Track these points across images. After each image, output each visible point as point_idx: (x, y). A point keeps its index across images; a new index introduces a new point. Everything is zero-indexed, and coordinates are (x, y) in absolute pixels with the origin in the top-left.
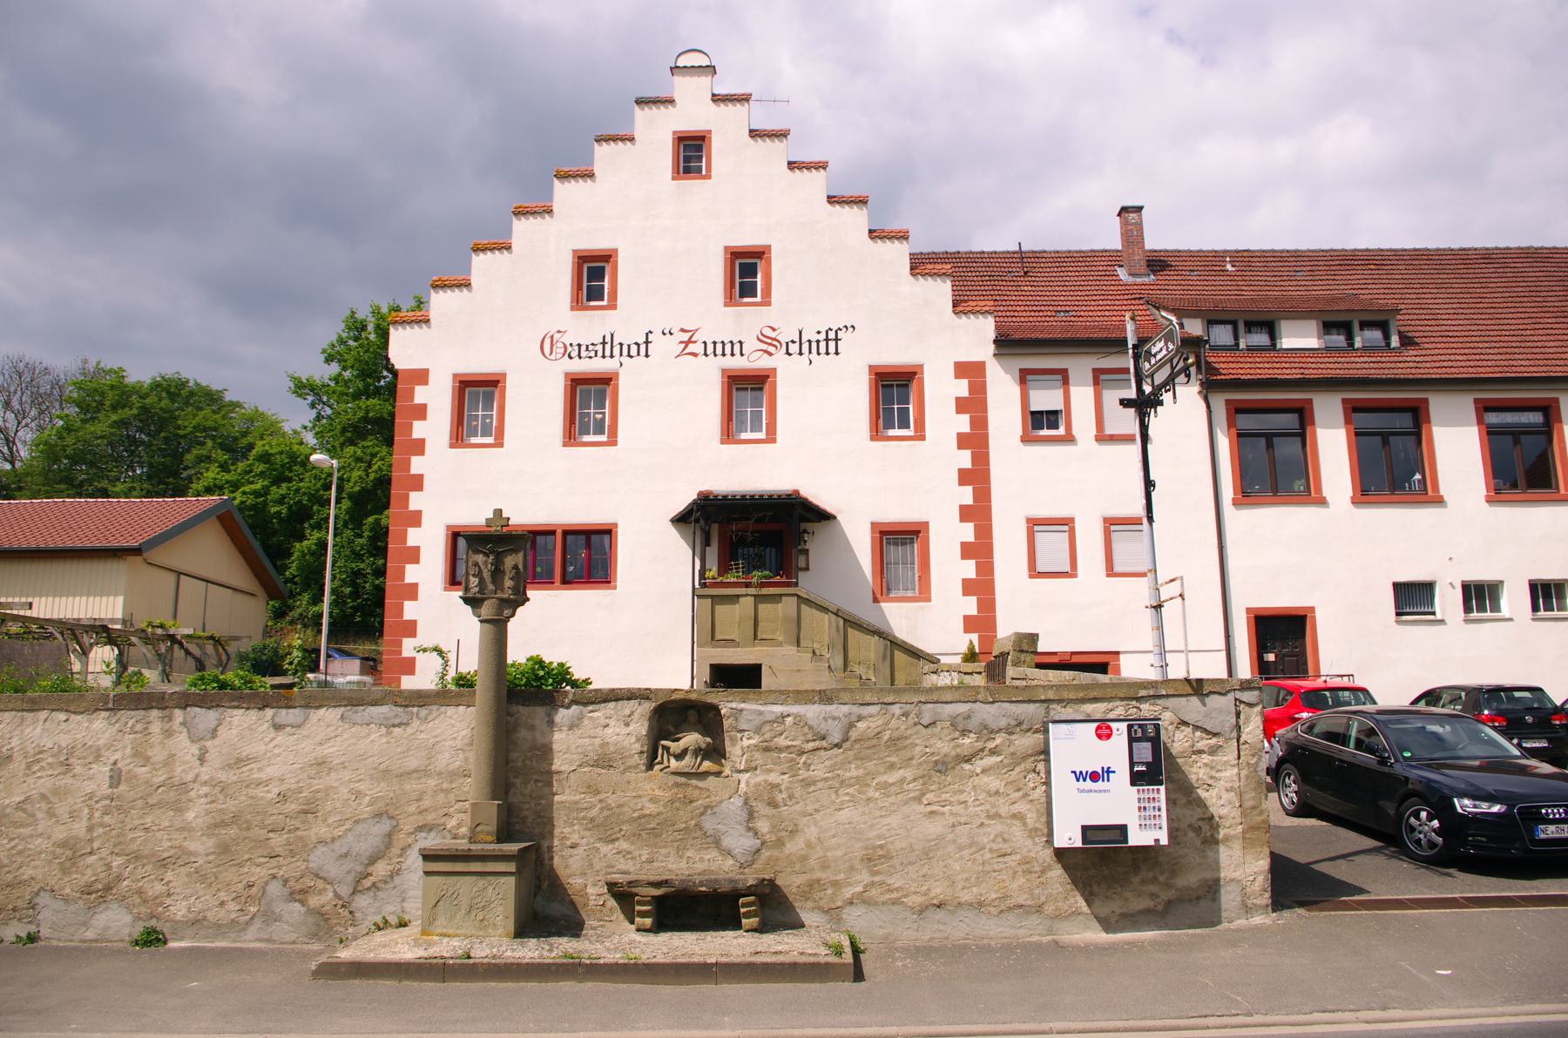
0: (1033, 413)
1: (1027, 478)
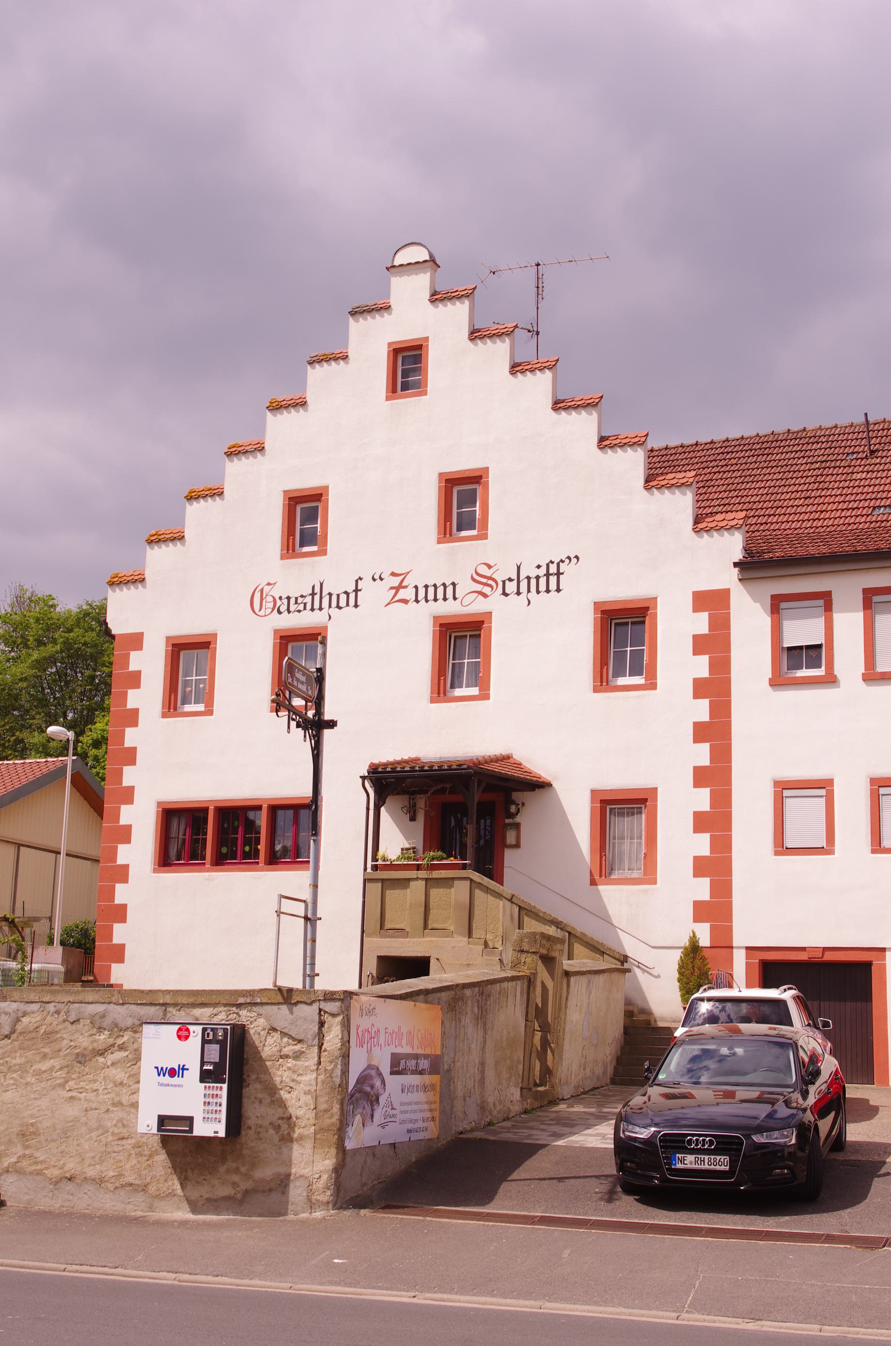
1: (774, 729)
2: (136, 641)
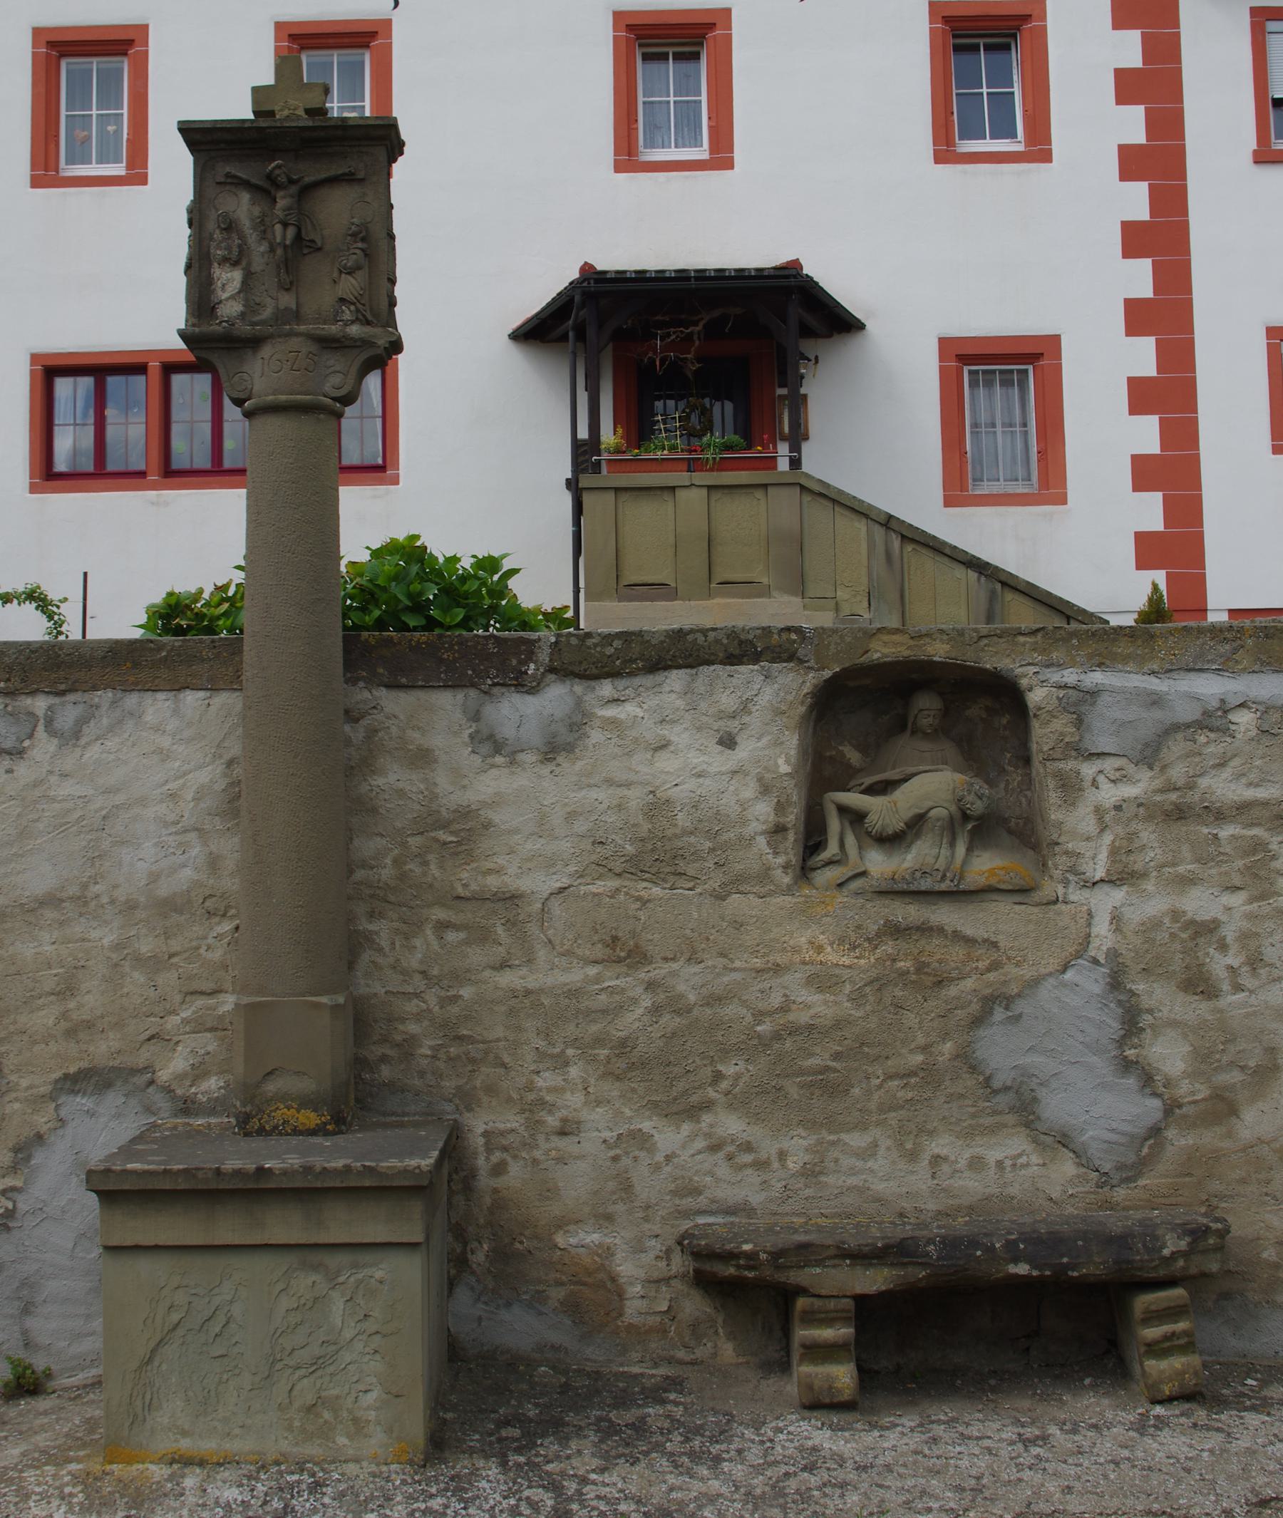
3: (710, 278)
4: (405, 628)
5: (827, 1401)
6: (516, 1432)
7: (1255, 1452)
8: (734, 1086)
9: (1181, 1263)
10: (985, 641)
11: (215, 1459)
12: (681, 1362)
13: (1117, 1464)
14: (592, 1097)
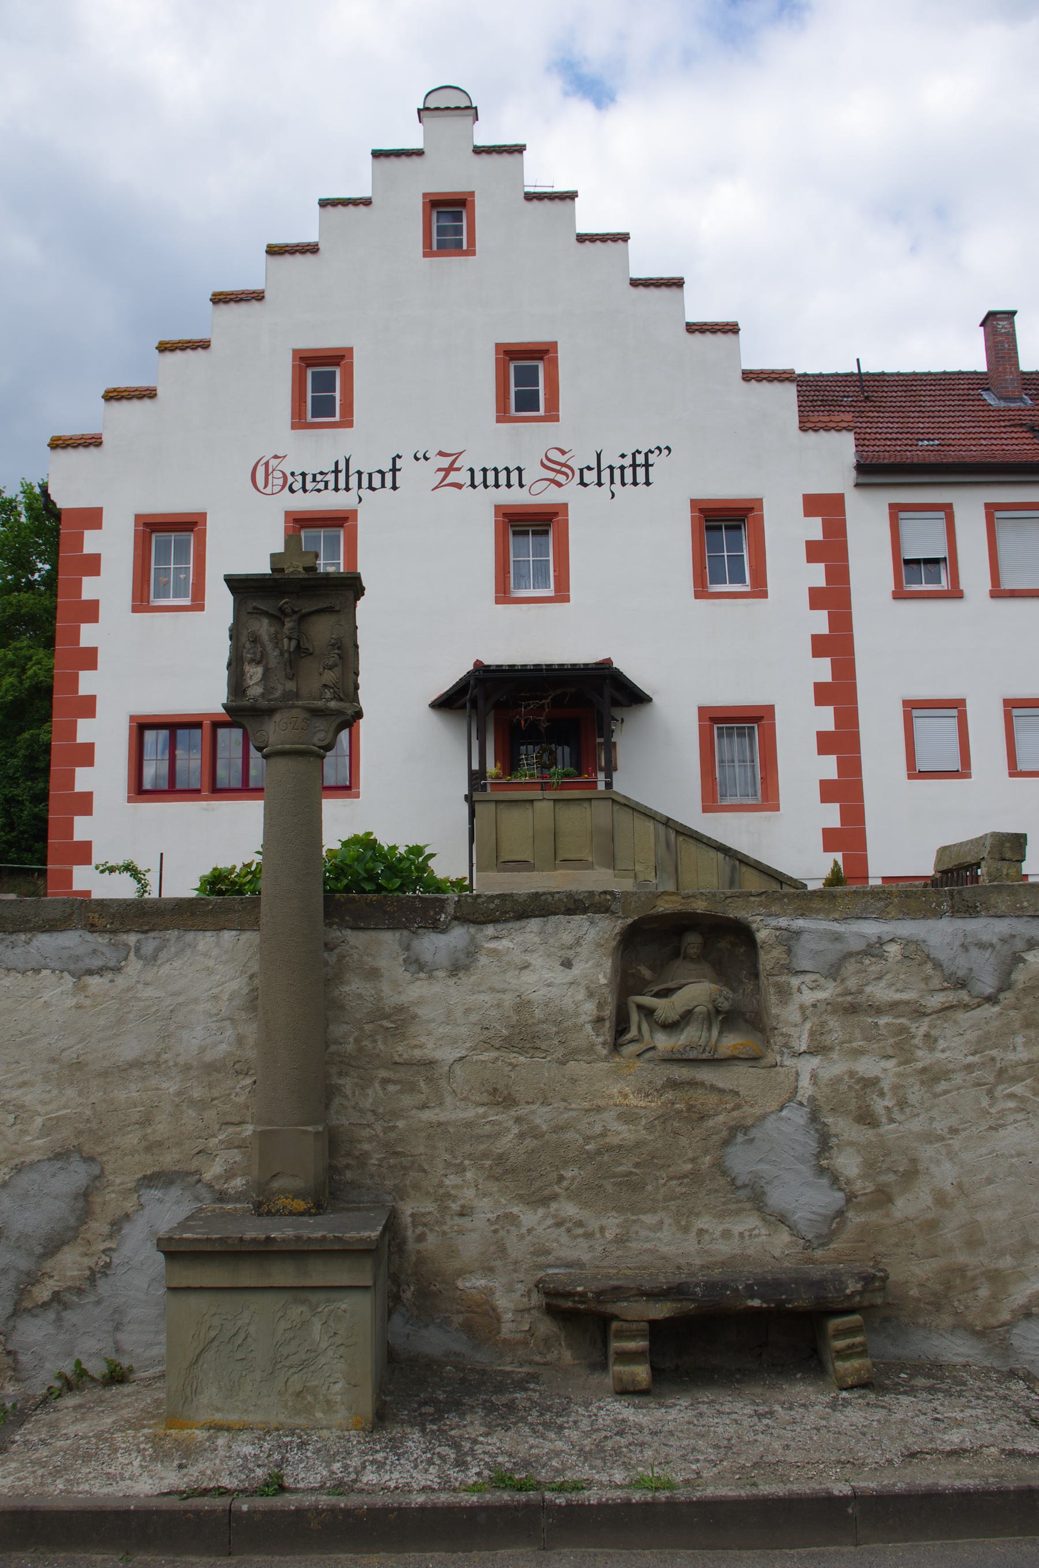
0: (907, 562)
1: (901, 647)
2: (93, 518)
3: (555, 670)
4: (363, 891)
5: (632, 1389)
6: (431, 1410)
7: (906, 1421)
8: (571, 1184)
9: (858, 1298)
10: (730, 900)
11: (237, 1427)
12: (537, 1364)
13: (818, 1430)
14: (481, 1192)
